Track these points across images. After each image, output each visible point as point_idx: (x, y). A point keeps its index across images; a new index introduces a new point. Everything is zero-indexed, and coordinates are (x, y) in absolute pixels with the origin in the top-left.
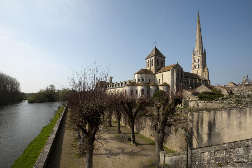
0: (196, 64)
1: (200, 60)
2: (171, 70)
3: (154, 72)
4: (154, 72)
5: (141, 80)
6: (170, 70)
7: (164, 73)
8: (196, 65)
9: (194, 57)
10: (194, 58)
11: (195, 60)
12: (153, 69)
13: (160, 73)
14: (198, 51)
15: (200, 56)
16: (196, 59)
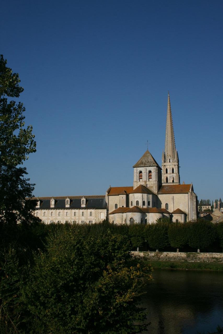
0: (168, 176)
1: (175, 170)
2: (189, 193)
3: (155, 190)
4: (155, 190)
5: (146, 204)
6: (188, 193)
7: (175, 195)
8: (168, 177)
9: (165, 164)
10: (165, 166)
11: (167, 170)
12: (152, 187)
13: (170, 195)
14: (171, 156)
15: (175, 165)
16: (168, 167)
